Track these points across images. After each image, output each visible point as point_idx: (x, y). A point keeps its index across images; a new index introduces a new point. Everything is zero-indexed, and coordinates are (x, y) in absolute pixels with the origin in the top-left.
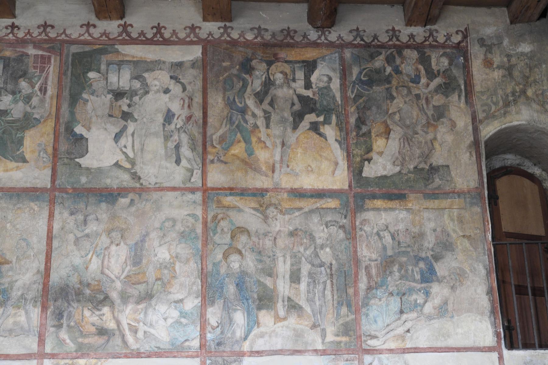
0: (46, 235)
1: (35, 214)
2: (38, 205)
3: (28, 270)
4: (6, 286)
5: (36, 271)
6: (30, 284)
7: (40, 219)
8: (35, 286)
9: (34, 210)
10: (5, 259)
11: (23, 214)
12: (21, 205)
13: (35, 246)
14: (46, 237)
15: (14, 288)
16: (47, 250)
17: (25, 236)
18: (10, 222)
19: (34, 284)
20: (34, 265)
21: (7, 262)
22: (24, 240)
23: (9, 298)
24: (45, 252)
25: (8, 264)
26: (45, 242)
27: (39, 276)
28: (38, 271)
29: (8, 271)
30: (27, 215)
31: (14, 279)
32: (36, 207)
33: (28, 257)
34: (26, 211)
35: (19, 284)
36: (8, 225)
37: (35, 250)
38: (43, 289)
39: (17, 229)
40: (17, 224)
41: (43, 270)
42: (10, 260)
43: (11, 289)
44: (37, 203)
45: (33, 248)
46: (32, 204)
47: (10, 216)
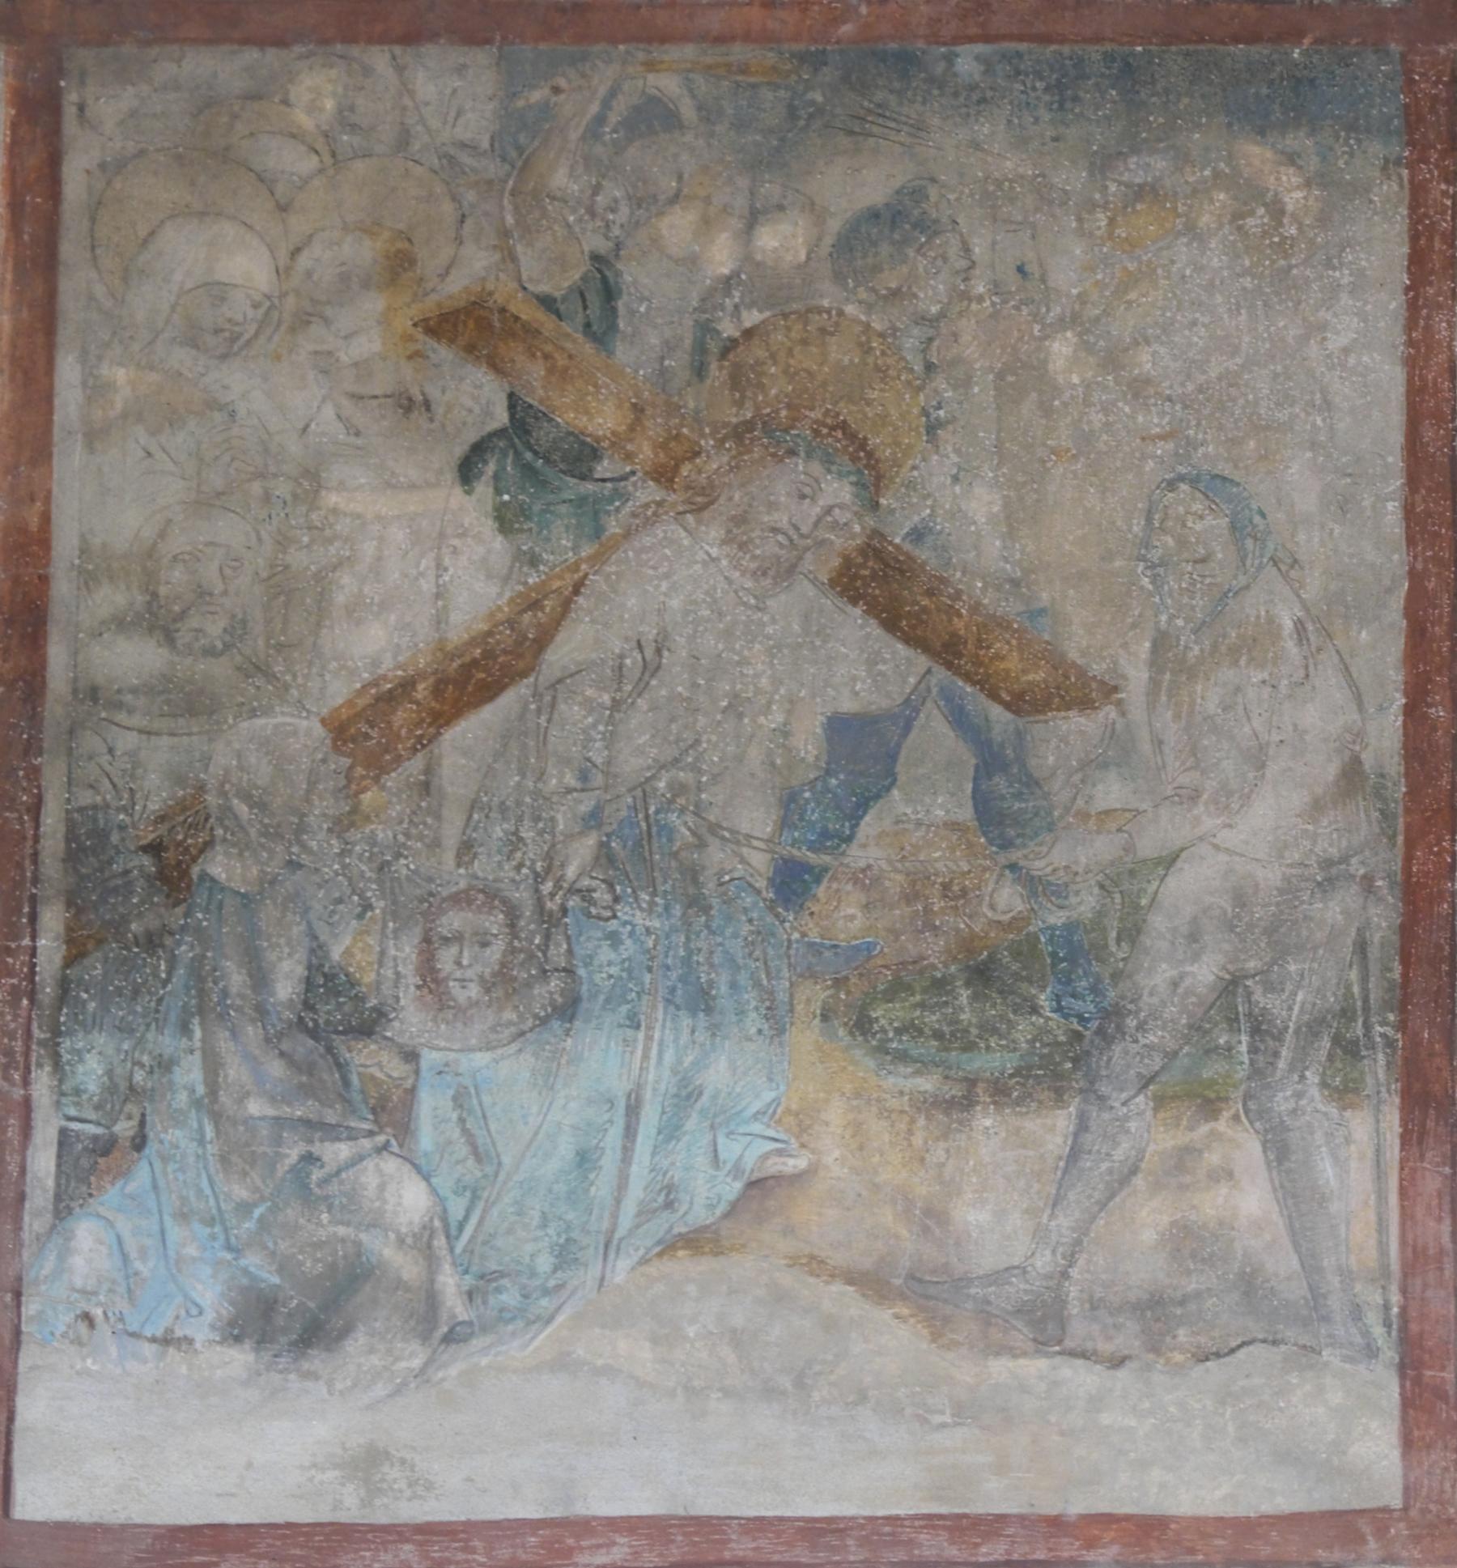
0: (1396, 438)
1: (1284, 247)
2: (1313, 163)
3: (1258, 758)
4: (1085, 903)
5: (1332, 770)
6: (1289, 890)
7: (1335, 288)
8: (1334, 910)
9: (1277, 211)
10: (1056, 660)
11: (1183, 251)
12: (1159, 164)
13: (1308, 543)
14: (1395, 460)
15: (1158, 921)
16: (1415, 577)
17: (1210, 453)
18: (1072, 320)
19: (1326, 887)
20: (1311, 716)
21: (1079, 691)
22: (1213, 486)
23: (1113, 1014)
24: (1397, 602)
25: (1085, 704)
26: (1393, 507)
27: (1363, 820)
28: (1352, 776)
29: (1092, 766)
30: (1216, 261)
31: (1147, 847)
32: (1291, 176)
33: (1255, 645)
34: (1205, 220)
35: (1190, 886)
36: (1061, 348)
37: (1313, 587)
38: (1407, 931)
39: (1139, 389)
40: (1142, 339)
41: (1394, 766)
42: (1097, 669)
43: (1132, 933)
44: (1298, 140)
45: (1288, 564)
46: (1256, 154)
47: (1068, 268)
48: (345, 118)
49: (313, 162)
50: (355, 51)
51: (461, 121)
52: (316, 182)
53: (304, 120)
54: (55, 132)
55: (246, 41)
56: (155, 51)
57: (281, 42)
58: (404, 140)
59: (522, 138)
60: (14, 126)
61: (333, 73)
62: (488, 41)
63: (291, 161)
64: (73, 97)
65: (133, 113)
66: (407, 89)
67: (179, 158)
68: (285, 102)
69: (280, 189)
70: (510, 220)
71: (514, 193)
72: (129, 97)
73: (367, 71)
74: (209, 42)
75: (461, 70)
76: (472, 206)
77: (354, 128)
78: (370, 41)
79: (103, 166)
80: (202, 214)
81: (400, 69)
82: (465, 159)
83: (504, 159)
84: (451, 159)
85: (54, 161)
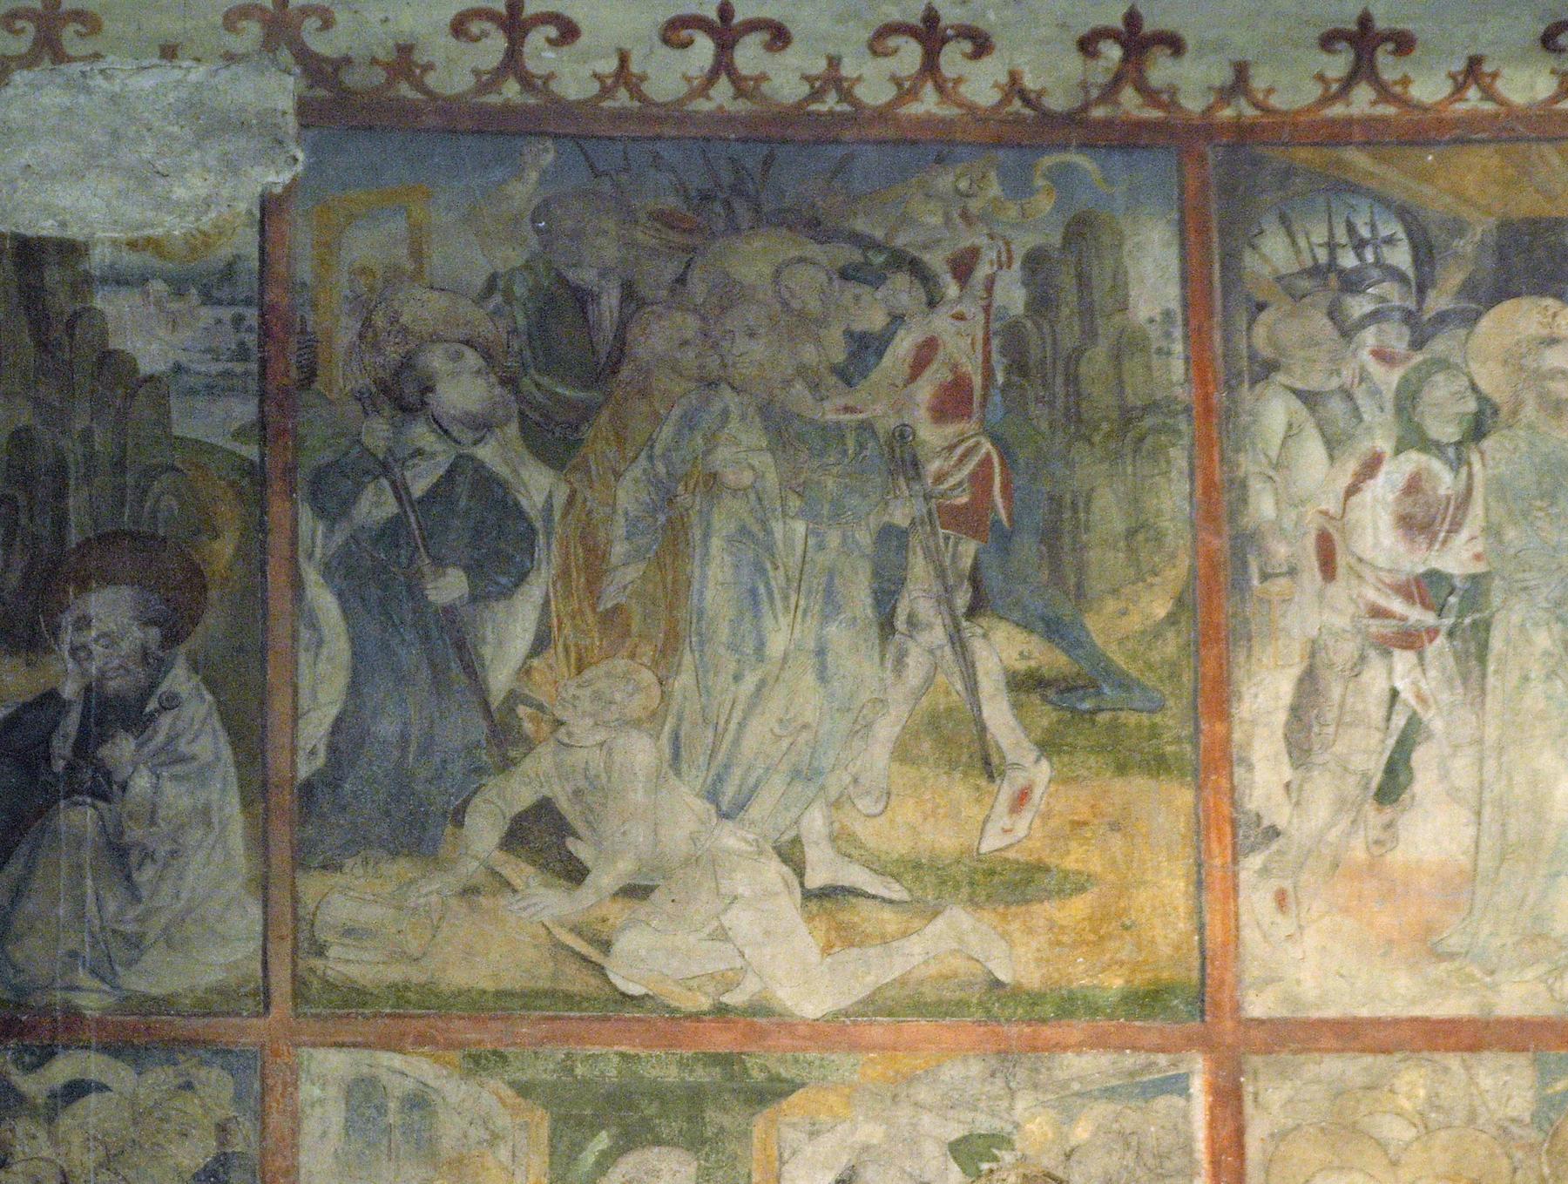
48: (1433, 1103)
49: (1411, 1133)
50: (1437, 1056)
51: (1512, 1103)
52: (1415, 1146)
53: (1407, 1105)
54: (1239, 1111)
55: (1363, 1051)
56: (1302, 1058)
57: (1386, 1051)
58: (1472, 1118)
59: (1552, 1115)
60: (1212, 1108)
61: (1423, 1071)
62: (1525, 1049)
63: (1397, 1131)
64: (1251, 1089)
65: (1290, 1100)
66: (1472, 1080)
67: (1322, 1129)
68: (1391, 1091)
69: (1392, 1151)
70: (1546, 1171)
71: (1549, 1151)
72: (1287, 1089)
73: (1446, 1070)
74: (1338, 1051)
75: (1509, 1068)
76: (1521, 1161)
77: (1438, 1108)
78: (1447, 1050)
79: (1272, 1135)
80: (1341, 1168)
81: (1468, 1068)
82: (1515, 1129)
83: (1540, 1128)
84: (1505, 1130)
85: (1239, 1133)
